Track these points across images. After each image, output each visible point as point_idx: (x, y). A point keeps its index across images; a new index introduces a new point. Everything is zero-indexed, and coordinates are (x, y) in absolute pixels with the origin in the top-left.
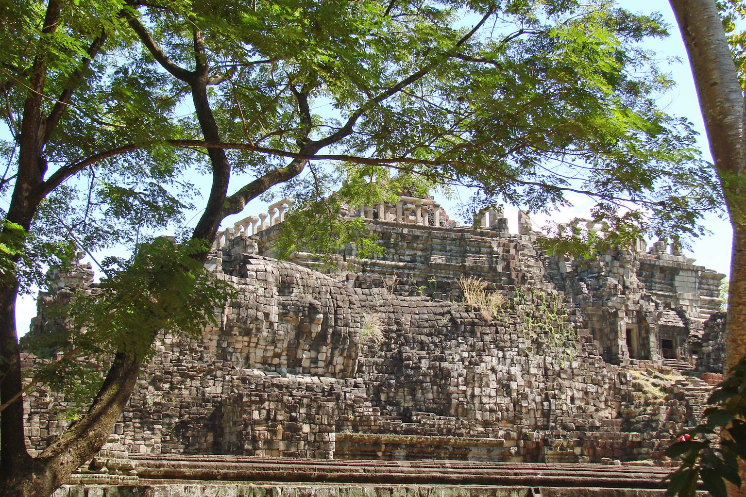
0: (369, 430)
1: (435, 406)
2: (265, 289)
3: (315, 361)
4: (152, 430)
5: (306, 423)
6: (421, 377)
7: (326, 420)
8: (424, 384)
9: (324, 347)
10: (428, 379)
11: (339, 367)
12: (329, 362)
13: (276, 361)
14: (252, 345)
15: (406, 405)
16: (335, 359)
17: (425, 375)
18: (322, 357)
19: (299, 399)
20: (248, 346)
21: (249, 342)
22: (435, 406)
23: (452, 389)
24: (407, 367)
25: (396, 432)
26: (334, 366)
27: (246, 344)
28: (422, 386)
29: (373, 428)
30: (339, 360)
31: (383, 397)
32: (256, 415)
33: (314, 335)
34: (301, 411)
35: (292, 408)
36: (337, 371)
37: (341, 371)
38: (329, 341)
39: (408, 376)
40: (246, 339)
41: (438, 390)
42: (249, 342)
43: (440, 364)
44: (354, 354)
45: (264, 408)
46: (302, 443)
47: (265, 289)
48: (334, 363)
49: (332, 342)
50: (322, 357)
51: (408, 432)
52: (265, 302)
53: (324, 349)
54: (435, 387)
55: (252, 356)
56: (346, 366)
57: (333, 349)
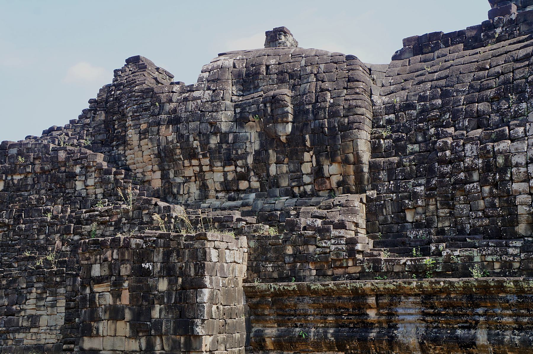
0: (345, 273)
1: (486, 221)
2: (214, 91)
3: (296, 176)
4: (54, 294)
5: (163, 277)
6: (462, 175)
7: (192, 269)
8: (468, 186)
9: (306, 154)
10: (476, 176)
11: (335, 180)
12: (318, 173)
13: (243, 185)
14: (205, 168)
15: (440, 225)
16: (325, 167)
17: (469, 170)
18: (306, 168)
19: (154, 241)
20: (201, 170)
21: (200, 166)
22: (486, 221)
23: (515, 186)
24: (443, 161)
25: (397, 275)
26: (328, 178)
27: (197, 169)
28: (464, 190)
29: (351, 270)
30: (333, 171)
31: (409, 217)
32: (96, 271)
33: (283, 139)
34: (155, 259)
35: (144, 254)
36: (334, 185)
37: (339, 184)
38: (308, 144)
39: (443, 175)
40: (195, 162)
41: (491, 192)
42: (200, 166)
43: (493, 147)
44: (351, 156)
45: (106, 260)
46: (158, 307)
47: (214, 91)
48: (326, 174)
49: (312, 143)
50: (306, 168)
51: (419, 272)
52: (210, 109)
53: (307, 156)
54: (487, 189)
55: (209, 183)
56: (345, 175)
57: (318, 154)
